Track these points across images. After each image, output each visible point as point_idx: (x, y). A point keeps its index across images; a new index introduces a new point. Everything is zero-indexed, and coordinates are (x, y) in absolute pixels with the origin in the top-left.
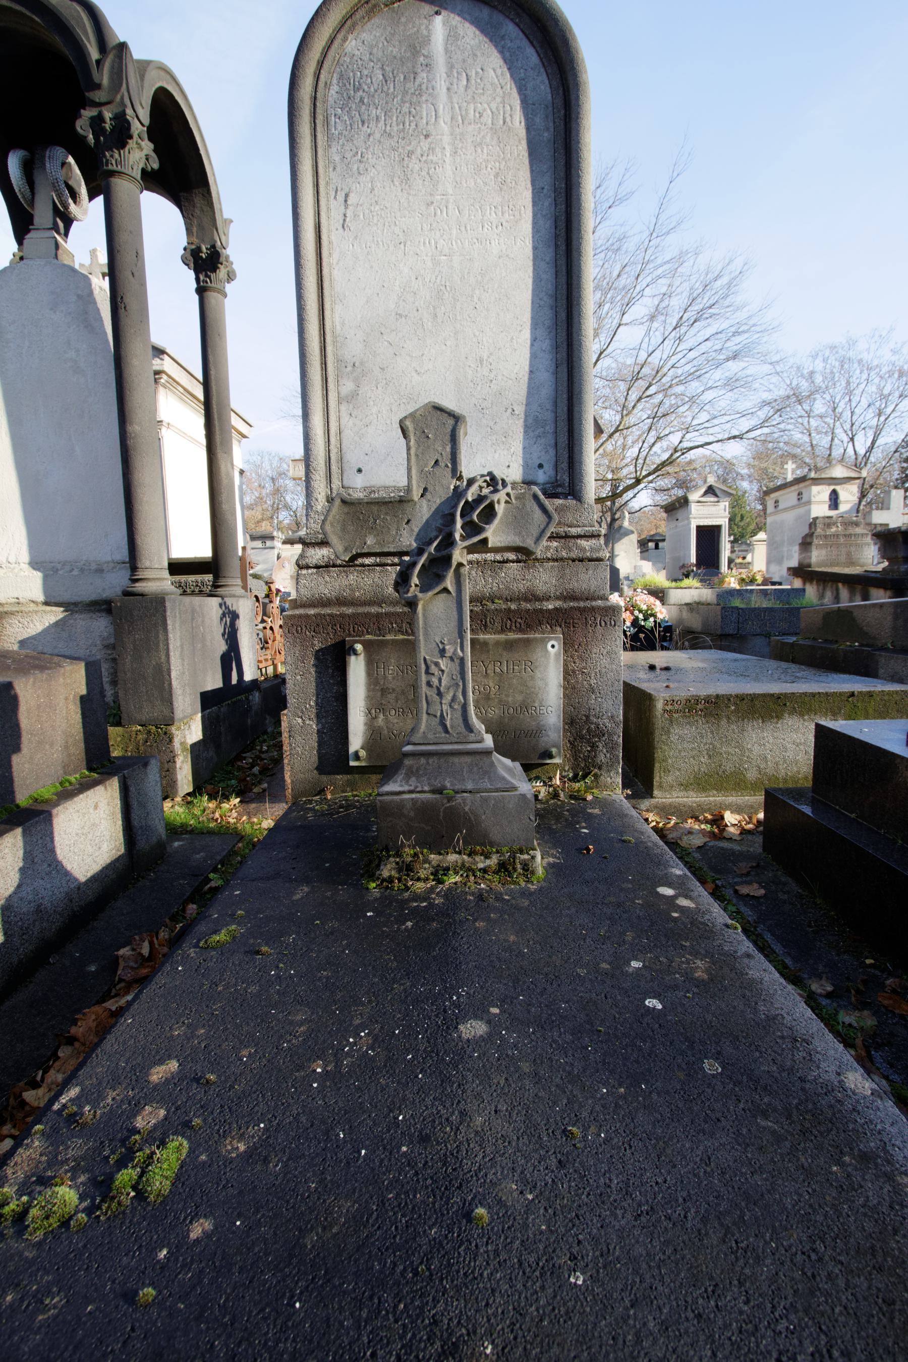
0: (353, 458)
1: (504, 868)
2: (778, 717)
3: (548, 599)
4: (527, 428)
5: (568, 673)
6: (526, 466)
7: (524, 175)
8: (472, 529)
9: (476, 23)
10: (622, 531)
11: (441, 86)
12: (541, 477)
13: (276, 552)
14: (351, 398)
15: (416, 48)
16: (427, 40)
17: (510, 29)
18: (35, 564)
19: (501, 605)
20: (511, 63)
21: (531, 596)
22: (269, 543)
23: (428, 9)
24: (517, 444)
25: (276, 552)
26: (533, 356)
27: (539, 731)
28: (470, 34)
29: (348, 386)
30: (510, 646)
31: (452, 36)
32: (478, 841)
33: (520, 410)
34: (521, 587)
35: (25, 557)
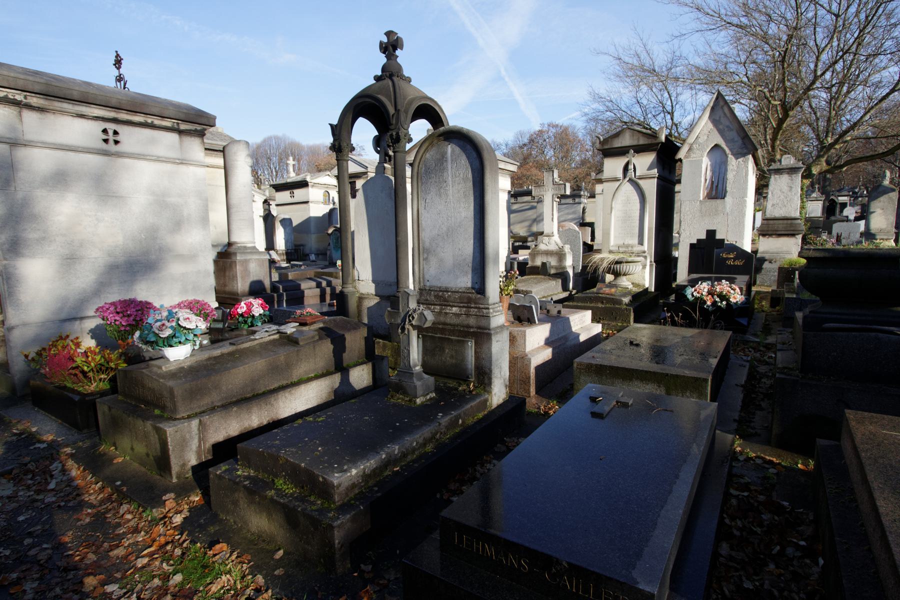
0: (427, 277)
1: (410, 401)
2: (631, 380)
3: (472, 327)
4: (473, 271)
5: (476, 352)
6: (473, 283)
7: (472, 192)
8: (410, 321)
9: (460, 146)
10: (880, 189)
11: (449, 167)
12: (477, 286)
13: (582, 206)
14: (426, 259)
15: (442, 159)
16: (446, 153)
17: (469, 147)
18: (373, 281)
19: (459, 328)
20: (468, 158)
21: (468, 326)
22: (577, 200)
23: (447, 143)
24: (470, 276)
25: (582, 206)
26: (474, 248)
27: (466, 369)
28: (458, 150)
29: (426, 255)
30: (459, 341)
31: (453, 151)
32: (405, 393)
33: (470, 265)
34: (466, 323)
35: (371, 279)
